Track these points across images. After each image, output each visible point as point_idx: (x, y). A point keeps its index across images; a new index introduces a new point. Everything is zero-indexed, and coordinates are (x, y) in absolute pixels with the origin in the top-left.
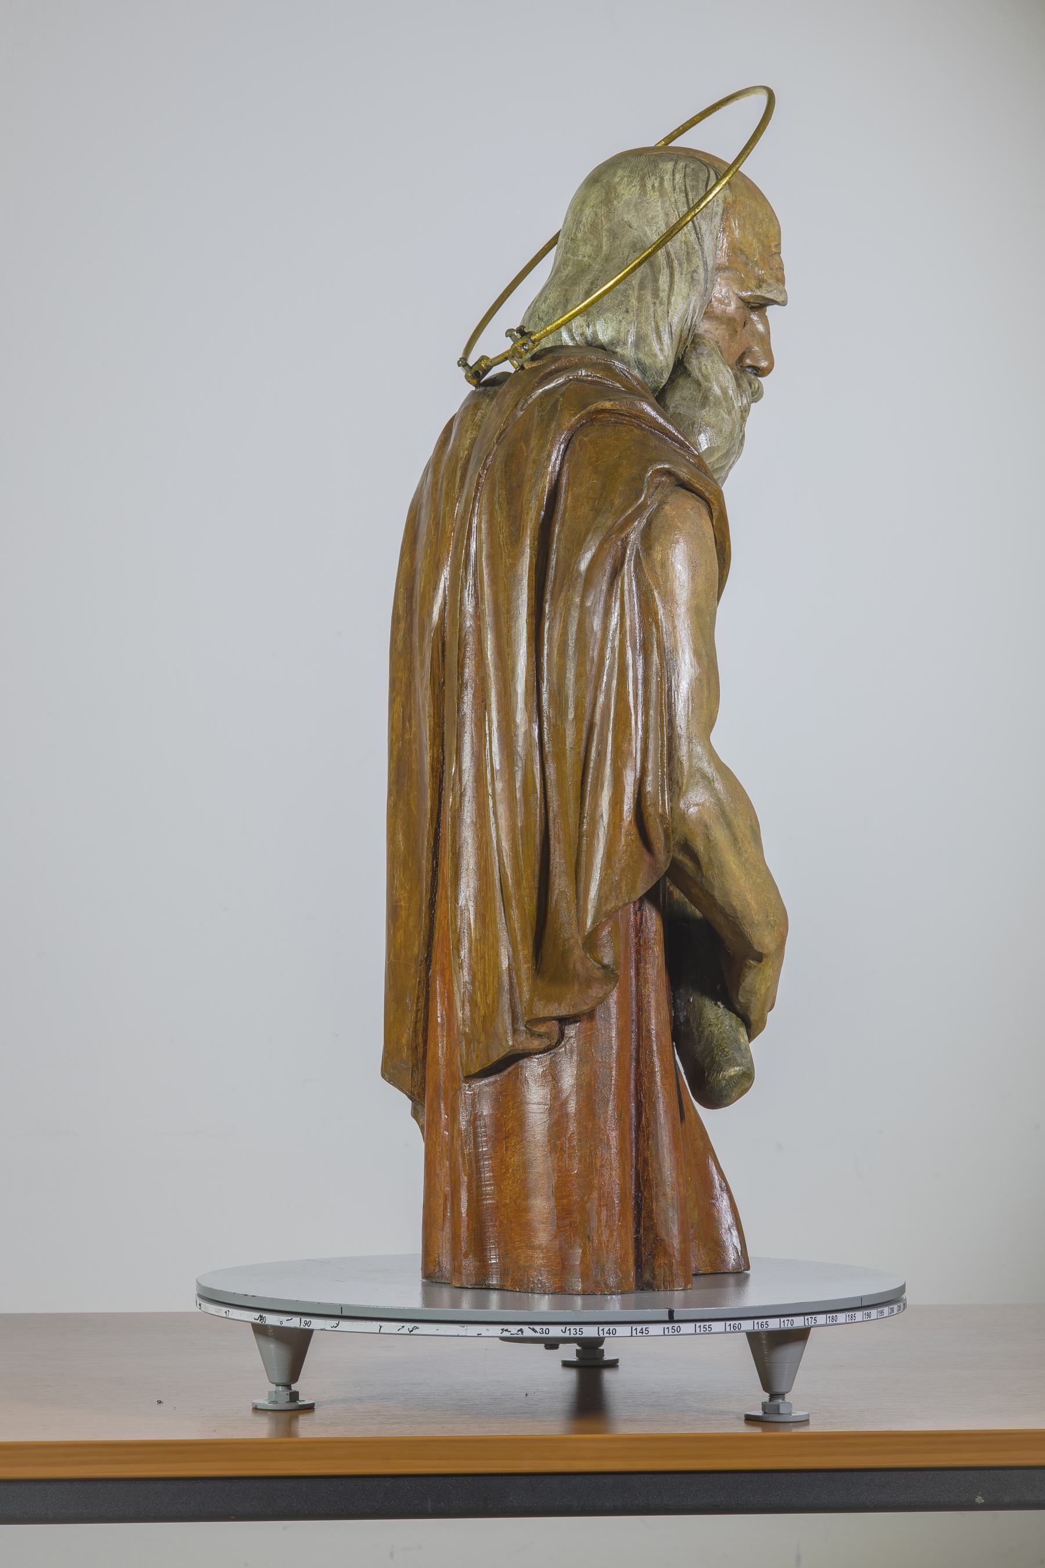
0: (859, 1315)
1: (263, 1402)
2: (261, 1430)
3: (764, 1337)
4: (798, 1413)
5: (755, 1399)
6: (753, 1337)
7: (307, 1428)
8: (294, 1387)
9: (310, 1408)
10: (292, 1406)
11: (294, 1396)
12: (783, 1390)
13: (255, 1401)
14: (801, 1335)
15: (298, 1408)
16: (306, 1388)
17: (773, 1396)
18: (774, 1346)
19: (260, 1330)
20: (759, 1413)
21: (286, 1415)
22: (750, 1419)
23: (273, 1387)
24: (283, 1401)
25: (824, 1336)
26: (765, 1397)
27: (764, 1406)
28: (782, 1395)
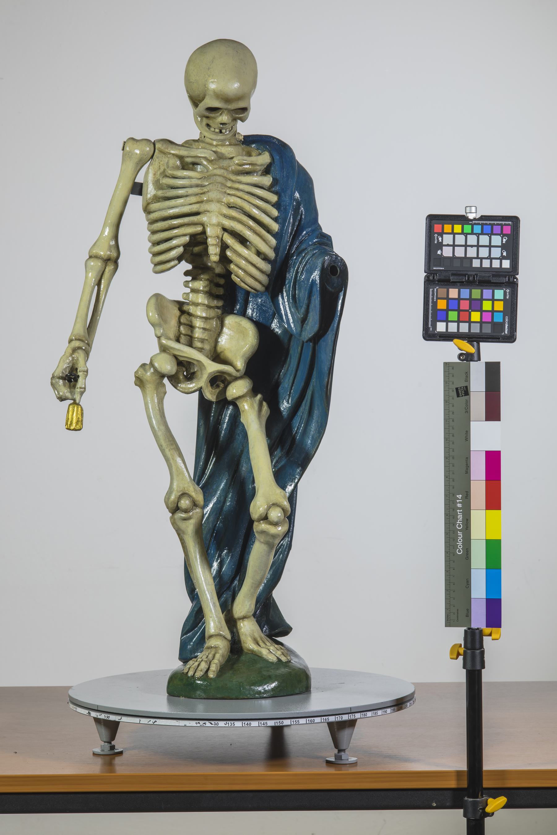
0: (380, 712)
1: (98, 750)
4: (353, 759)
10: (112, 752)
12: (344, 748)
13: (94, 750)
15: (111, 755)
17: (340, 751)
18: (340, 727)
20: (332, 759)
21: (107, 758)
22: (328, 762)
24: (107, 751)
26: (336, 751)
27: (336, 756)
28: (344, 750)
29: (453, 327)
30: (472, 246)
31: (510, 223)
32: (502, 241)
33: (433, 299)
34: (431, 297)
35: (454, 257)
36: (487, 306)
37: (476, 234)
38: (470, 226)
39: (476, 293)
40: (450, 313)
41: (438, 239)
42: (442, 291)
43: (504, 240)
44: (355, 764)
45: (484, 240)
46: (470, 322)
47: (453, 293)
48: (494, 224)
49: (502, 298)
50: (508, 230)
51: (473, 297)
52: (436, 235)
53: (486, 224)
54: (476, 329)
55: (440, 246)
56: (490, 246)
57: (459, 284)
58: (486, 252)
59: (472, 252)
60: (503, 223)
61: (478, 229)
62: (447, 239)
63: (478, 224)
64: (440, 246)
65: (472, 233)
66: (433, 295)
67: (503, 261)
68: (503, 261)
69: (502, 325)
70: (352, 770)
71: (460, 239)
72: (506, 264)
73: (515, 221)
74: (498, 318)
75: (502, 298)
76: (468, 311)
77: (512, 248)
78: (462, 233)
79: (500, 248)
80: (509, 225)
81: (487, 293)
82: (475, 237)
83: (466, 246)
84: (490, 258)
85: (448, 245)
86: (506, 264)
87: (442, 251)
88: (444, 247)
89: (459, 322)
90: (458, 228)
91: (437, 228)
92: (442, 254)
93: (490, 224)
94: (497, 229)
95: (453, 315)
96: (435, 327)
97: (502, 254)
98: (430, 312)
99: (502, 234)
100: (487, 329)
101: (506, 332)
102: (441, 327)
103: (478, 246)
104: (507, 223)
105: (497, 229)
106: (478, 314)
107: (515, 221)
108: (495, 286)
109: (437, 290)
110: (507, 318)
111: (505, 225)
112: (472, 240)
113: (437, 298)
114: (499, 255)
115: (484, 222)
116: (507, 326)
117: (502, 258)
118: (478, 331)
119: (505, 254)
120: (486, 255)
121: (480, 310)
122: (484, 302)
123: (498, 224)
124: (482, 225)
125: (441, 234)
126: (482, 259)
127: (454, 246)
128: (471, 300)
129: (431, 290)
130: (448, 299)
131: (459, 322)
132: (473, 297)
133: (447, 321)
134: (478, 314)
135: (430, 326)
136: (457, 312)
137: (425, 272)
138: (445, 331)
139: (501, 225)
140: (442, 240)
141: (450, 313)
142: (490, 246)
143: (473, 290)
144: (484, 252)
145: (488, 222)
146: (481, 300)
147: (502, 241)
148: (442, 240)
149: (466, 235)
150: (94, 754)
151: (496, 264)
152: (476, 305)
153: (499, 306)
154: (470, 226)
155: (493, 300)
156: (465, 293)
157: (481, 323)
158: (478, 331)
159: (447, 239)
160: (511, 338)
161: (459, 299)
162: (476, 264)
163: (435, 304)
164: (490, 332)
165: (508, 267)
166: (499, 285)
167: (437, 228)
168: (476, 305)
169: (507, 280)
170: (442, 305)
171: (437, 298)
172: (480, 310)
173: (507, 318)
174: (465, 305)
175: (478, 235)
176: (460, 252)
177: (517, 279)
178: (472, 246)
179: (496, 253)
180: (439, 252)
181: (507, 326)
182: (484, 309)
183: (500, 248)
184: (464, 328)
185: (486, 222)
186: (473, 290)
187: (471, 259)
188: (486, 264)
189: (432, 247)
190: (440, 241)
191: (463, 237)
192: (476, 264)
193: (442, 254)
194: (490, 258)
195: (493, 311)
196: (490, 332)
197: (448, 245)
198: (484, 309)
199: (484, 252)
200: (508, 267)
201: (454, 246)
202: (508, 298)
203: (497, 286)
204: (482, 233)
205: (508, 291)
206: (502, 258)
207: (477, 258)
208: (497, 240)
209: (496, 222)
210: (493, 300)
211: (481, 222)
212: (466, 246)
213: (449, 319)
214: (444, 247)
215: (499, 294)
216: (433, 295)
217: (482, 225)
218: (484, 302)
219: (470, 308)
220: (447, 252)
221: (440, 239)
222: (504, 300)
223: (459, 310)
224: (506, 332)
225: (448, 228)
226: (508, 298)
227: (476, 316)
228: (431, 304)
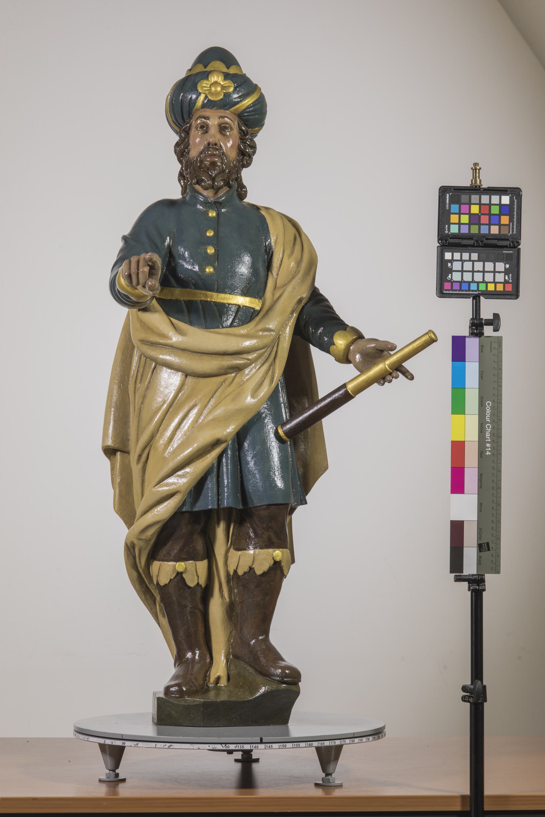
29: (495, 199)
30: (478, 271)
31: (445, 292)
32: (452, 276)
33: (513, 225)
34: (515, 226)
35: (494, 261)
36: (465, 219)
37: (475, 282)
38: (480, 289)
39: (474, 230)
40: (498, 212)
41: (509, 278)
42: (505, 231)
43: (450, 276)
45: (468, 277)
46: (480, 204)
47: (495, 230)
48: (459, 291)
49: (451, 225)
50: (447, 286)
51: (477, 226)
52: (511, 281)
53: (466, 291)
54: (475, 198)
55: (506, 272)
56: (462, 271)
57: (490, 237)
58: (467, 267)
59: (479, 266)
60: (451, 292)
61: (473, 287)
62: (500, 278)
63: (473, 291)
64: (506, 272)
65: (478, 283)
66: (513, 228)
67: (451, 258)
68: (451, 258)
69: (451, 202)
71: (489, 277)
72: (448, 256)
73: (441, 293)
74: (455, 208)
75: (451, 225)
76: (482, 214)
77: (444, 269)
78: (487, 283)
79: (453, 269)
80: (446, 290)
81: (465, 230)
82: (476, 279)
83: (484, 272)
84: (462, 261)
85: (500, 272)
86: (448, 256)
87: (505, 268)
88: (503, 270)
89: (490, 205)
90: (491, 287)
91: (509, 288)
92: (505, 265)
93: (463, 291)
94: (456, 286)
95: (495, 210)
96: (511, 200)
97: (452, 265)
98: (515, 213)
99: (452, 282)
100: (464, 198)
101: (448, 195)
102: (506, 200)
103: (473, 271)
104: (448, 292)
105: (456, 286)
106: (472, 212)
107: (441, 293)
108: (458, 236)
109: (509, 232)
110: (447, 208)
111: (449, 290)
112: (478, 277)
113: (509, 225)
114: (455, 263)
115: (468, 293)
116: (447, 201)
117: (452, 261)
118: (473, 196)
119: (449, 265)
120: (465, 263)
121: (471, 216)
122: (468, 222)
123: (456, 290)
124: (469, 290)
125: (505, 282)
126: (470, 260)
127: (494, 272)
128: (479, 224)
129: (515, 233)
130: (500, 225)
131: (490, 205)
132: (477, 226)
133: (501, 205)
134: (472, 212)
135: (516, 201)
136: (492, 213)
137: (520, 249)
138: (502, 197)
139: (453, 290)
140: (505, 277)
141: (498, 212)
142: (462, 271)
143: (477, 232)
144: (468, 266)
145: (464, 292)
146: (470, 224)
147: (452, 276)
148: (505, 277)
149: (484, 281)
151: (457, 256)
152: (475, 219)
153: (454, 218)
154: (480, 289)
155: (460, 224)
156: (484, 230)
157: (470, 204)
158: (473, 196)
159: (500, 278)
160: (443, 190)
161: (490, 225)
162: (475, 256)
163: (511, 220)
164: (462, 196)
165: (446, 253)
166: (454, 236)
167: (509, 288)
168: (475, 219)
169: (447, 242)
170: (505, 220)
171: (509, 225)
172: (471, 216)
173: (447, 208)
174: (485, 219)
175: (473, 281)
176: (489, 266)
177: (438, 242)
178: (478, 271)
179: (457, 266)
180: (507, 266)
181: (447, 201)
182: (468, 216)
183: (453, 269)
184: (485, 199)
185: (466, 293)
186: (477, 232)
187: (479, 260)
188: (466, 256)
189: (514, 271)
190: (506, 276)
191: (486, 280)
192: (475, 256)
193: (505, 265)
194: (462, 261)
195: (460, 214)
196: (462, 196)
197: (500, 272)
198: (468, 216)
199: (468, 266)
200: (446, 253)
201: (494, 272)
202: (447, 226)
203: (456, 236)
204: (469, 283)
205: (447, 232)
206: (452, 261)
207: (473, 261)
208: (456, 277)
209: (458, 292)
210: (460, 224)
211: (471, 293)
212: (484, 272)
213: (498, 207)
214: (503, 270)
215: (454, 229)
216: (513, 228)
217: (469, 290)
218: (468, 222)
219: (480, 217)
220: (500, 266)
221: (507, 278)
222: (449, 224)
223: (490, 214)
224: (448, 195)
225: (500, 288)
226: (447, 226)
227: (475, 209)
228: (515, 220)
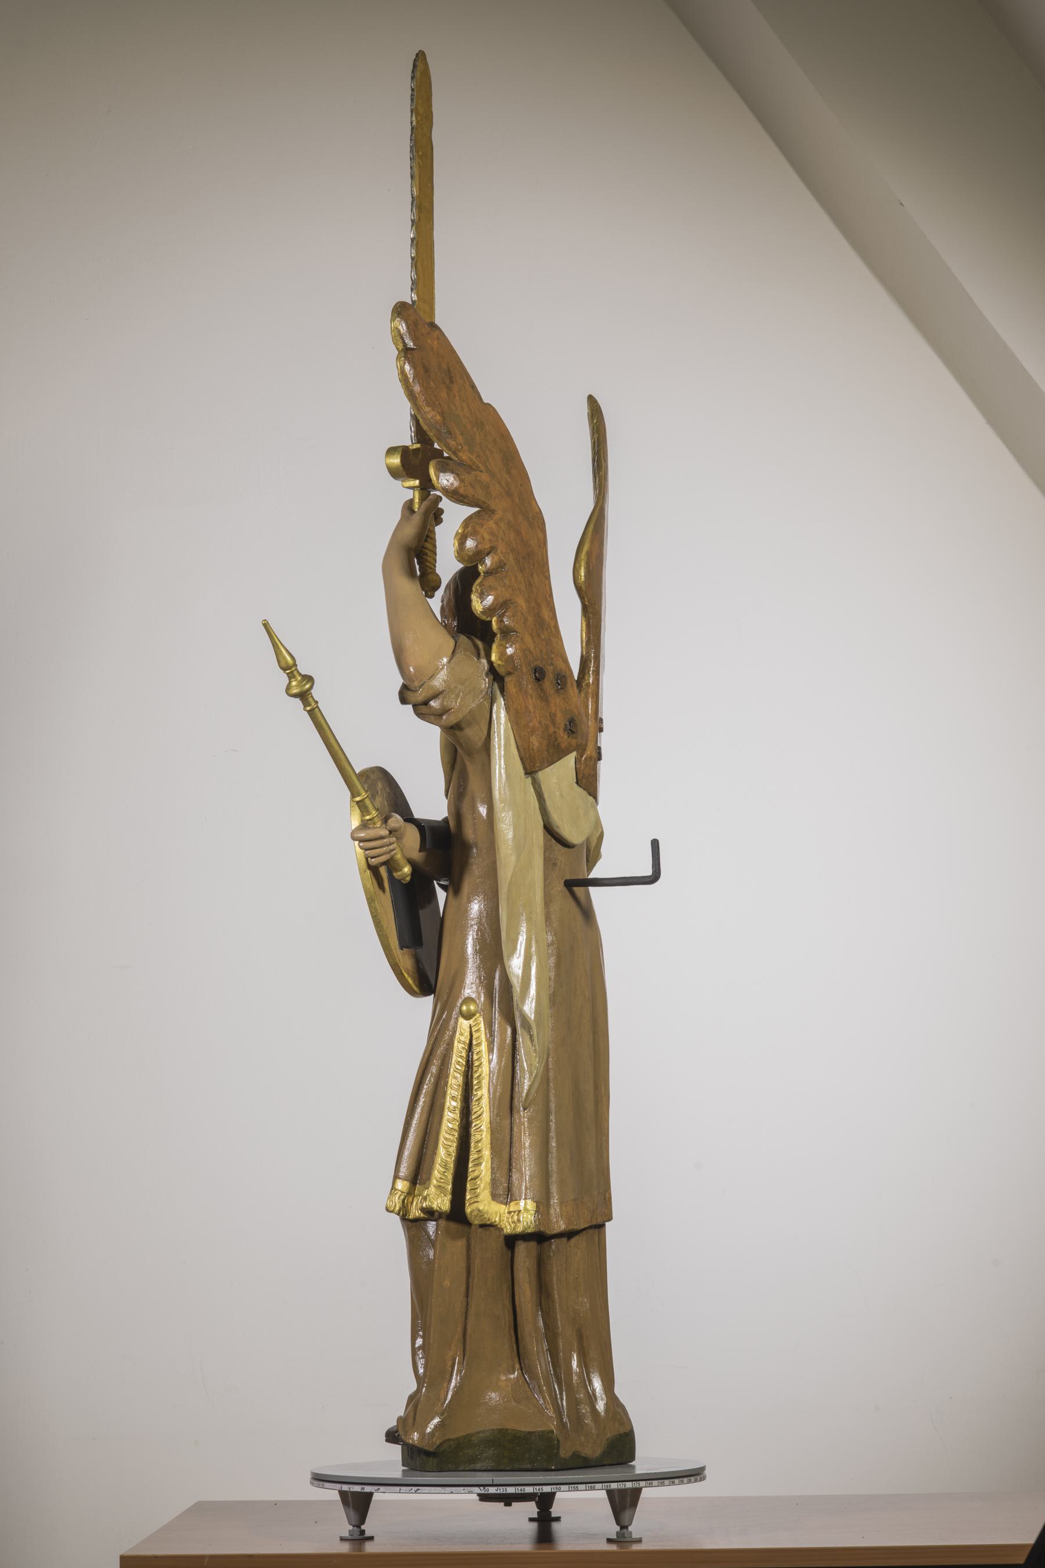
2: (345, 1548)
3: (616, 1493)
5: (613, 1529)
6: (610, 1493)
7: (370, 1548)
8: (363, 1527)
9: (371, 1538)
11: (363, 1532)
14: (637, 1492)
16: (368, 1528)
17: (622, 1528)
19: (342, 1493)
23: (351, 1527)
24: (356, 1536)
25: (649, 1493)
26: (618, 1528)
27: (617, 1533)
28: (626, 1527)
44: (639, 1541)
70: (635, 1547)
150: (342, 1539)
